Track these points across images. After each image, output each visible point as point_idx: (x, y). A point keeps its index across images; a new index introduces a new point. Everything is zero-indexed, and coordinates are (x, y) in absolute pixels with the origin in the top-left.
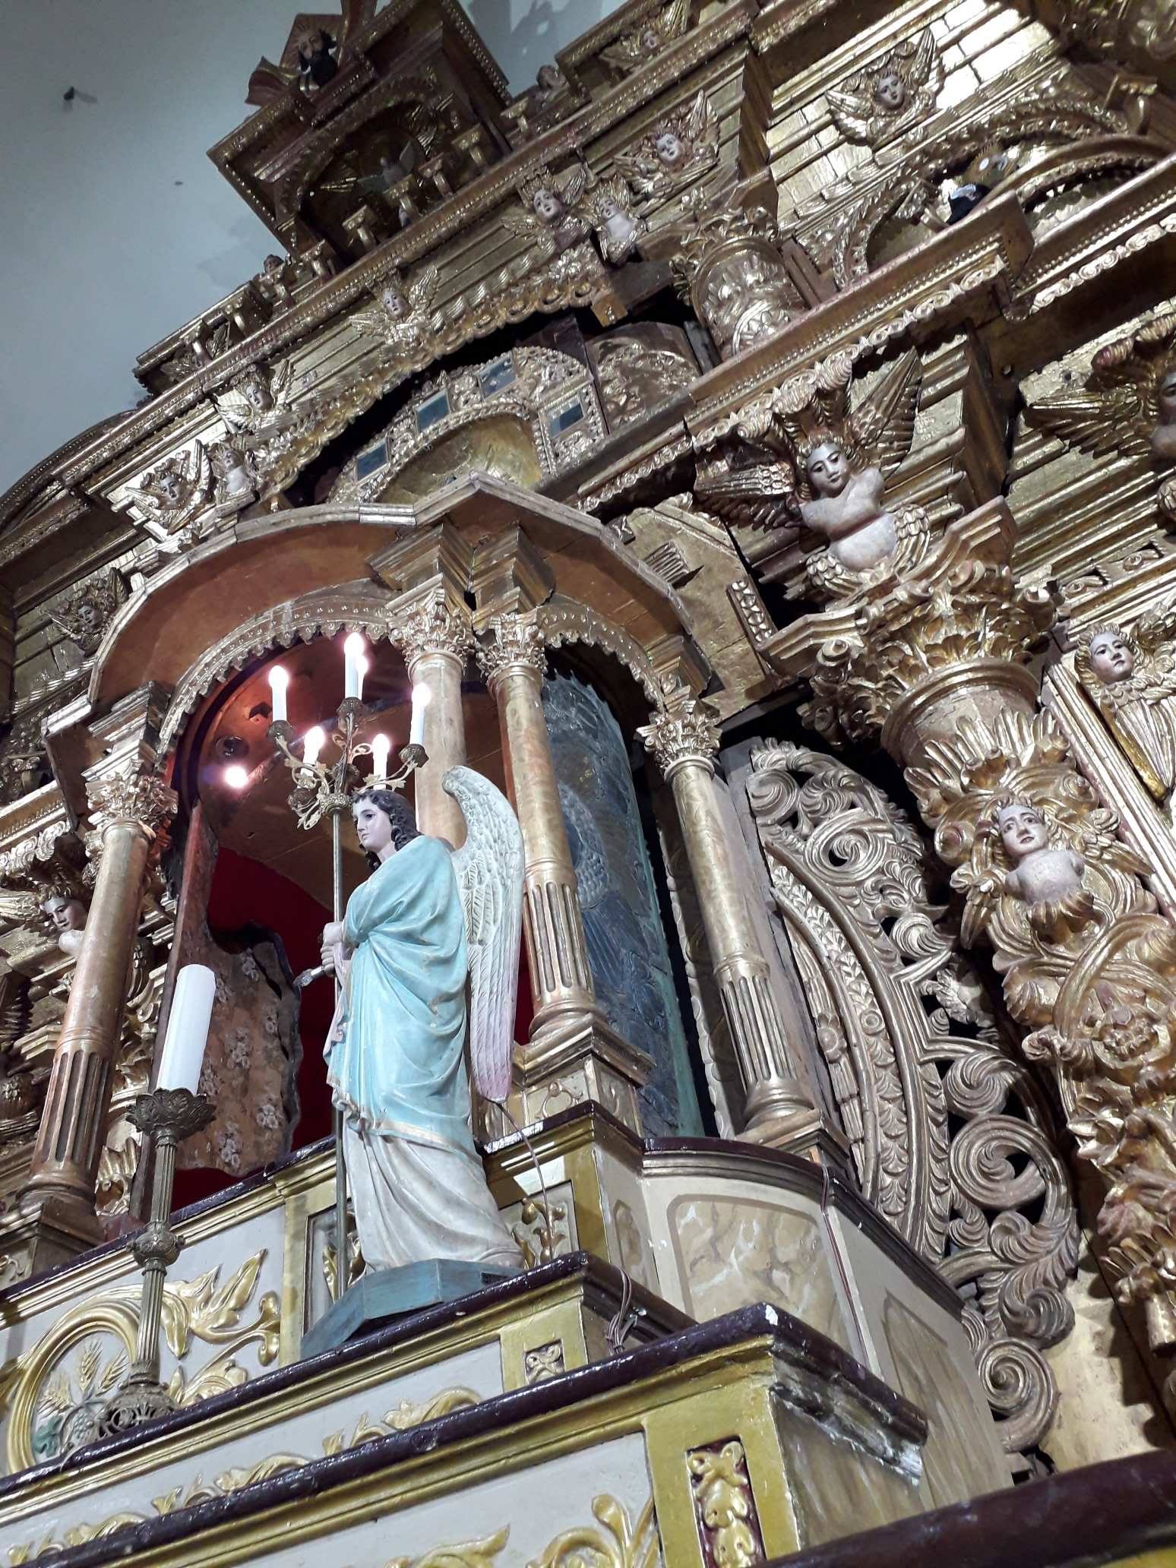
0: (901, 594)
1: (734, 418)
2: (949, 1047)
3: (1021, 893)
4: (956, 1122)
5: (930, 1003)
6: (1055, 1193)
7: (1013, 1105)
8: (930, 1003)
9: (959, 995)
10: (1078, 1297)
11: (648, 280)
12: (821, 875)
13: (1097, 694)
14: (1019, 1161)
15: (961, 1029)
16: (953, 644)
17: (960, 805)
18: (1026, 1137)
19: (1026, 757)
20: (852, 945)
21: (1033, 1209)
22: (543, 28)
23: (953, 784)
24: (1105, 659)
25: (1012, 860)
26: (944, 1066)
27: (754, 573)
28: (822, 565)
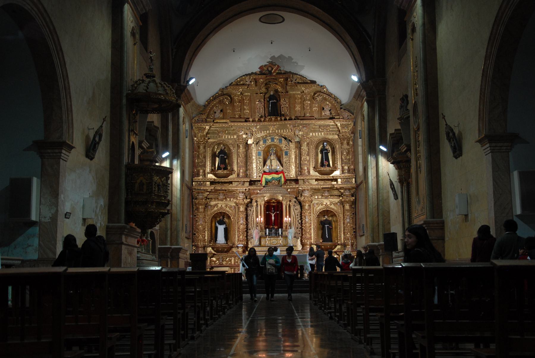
0: (306, 200)
1: (302, 187)
2: (298, 224)
3: (305, 220)
4: (297, 228)
5: (298, 221)
6: (301, 233)
7: (300, 228)
8: (298, 221)
9: (300, 221)
10: (300, 238)
11: (297, 139)
12: (295, 210)
13: (314, 206)
14: (299, 231)
15: (299, 223)
16: (307, 203)
17: (304, 213)
18: (300, 230)
19: (309, 212)
20: (295, 216)
21: (299, 233)
22: (296, 64)
23: (304, 212)
24: (315, 205)
25: (305, 218)
26: (298, 225)
27: (299, 192)
28: (303, 194)
